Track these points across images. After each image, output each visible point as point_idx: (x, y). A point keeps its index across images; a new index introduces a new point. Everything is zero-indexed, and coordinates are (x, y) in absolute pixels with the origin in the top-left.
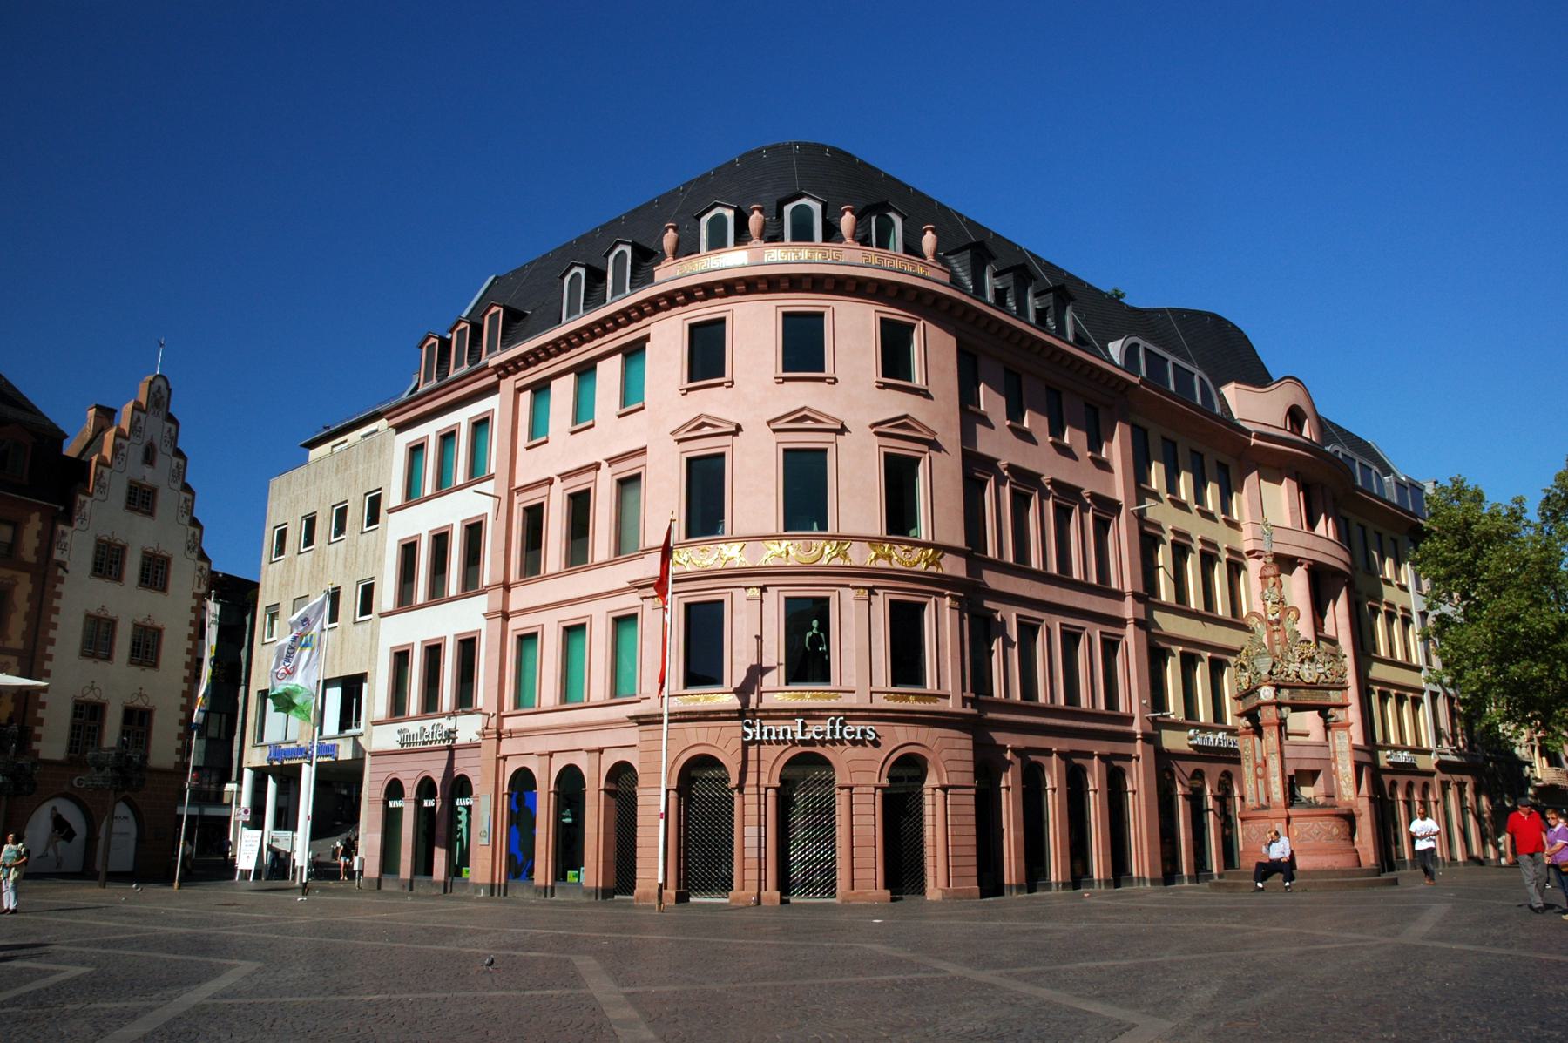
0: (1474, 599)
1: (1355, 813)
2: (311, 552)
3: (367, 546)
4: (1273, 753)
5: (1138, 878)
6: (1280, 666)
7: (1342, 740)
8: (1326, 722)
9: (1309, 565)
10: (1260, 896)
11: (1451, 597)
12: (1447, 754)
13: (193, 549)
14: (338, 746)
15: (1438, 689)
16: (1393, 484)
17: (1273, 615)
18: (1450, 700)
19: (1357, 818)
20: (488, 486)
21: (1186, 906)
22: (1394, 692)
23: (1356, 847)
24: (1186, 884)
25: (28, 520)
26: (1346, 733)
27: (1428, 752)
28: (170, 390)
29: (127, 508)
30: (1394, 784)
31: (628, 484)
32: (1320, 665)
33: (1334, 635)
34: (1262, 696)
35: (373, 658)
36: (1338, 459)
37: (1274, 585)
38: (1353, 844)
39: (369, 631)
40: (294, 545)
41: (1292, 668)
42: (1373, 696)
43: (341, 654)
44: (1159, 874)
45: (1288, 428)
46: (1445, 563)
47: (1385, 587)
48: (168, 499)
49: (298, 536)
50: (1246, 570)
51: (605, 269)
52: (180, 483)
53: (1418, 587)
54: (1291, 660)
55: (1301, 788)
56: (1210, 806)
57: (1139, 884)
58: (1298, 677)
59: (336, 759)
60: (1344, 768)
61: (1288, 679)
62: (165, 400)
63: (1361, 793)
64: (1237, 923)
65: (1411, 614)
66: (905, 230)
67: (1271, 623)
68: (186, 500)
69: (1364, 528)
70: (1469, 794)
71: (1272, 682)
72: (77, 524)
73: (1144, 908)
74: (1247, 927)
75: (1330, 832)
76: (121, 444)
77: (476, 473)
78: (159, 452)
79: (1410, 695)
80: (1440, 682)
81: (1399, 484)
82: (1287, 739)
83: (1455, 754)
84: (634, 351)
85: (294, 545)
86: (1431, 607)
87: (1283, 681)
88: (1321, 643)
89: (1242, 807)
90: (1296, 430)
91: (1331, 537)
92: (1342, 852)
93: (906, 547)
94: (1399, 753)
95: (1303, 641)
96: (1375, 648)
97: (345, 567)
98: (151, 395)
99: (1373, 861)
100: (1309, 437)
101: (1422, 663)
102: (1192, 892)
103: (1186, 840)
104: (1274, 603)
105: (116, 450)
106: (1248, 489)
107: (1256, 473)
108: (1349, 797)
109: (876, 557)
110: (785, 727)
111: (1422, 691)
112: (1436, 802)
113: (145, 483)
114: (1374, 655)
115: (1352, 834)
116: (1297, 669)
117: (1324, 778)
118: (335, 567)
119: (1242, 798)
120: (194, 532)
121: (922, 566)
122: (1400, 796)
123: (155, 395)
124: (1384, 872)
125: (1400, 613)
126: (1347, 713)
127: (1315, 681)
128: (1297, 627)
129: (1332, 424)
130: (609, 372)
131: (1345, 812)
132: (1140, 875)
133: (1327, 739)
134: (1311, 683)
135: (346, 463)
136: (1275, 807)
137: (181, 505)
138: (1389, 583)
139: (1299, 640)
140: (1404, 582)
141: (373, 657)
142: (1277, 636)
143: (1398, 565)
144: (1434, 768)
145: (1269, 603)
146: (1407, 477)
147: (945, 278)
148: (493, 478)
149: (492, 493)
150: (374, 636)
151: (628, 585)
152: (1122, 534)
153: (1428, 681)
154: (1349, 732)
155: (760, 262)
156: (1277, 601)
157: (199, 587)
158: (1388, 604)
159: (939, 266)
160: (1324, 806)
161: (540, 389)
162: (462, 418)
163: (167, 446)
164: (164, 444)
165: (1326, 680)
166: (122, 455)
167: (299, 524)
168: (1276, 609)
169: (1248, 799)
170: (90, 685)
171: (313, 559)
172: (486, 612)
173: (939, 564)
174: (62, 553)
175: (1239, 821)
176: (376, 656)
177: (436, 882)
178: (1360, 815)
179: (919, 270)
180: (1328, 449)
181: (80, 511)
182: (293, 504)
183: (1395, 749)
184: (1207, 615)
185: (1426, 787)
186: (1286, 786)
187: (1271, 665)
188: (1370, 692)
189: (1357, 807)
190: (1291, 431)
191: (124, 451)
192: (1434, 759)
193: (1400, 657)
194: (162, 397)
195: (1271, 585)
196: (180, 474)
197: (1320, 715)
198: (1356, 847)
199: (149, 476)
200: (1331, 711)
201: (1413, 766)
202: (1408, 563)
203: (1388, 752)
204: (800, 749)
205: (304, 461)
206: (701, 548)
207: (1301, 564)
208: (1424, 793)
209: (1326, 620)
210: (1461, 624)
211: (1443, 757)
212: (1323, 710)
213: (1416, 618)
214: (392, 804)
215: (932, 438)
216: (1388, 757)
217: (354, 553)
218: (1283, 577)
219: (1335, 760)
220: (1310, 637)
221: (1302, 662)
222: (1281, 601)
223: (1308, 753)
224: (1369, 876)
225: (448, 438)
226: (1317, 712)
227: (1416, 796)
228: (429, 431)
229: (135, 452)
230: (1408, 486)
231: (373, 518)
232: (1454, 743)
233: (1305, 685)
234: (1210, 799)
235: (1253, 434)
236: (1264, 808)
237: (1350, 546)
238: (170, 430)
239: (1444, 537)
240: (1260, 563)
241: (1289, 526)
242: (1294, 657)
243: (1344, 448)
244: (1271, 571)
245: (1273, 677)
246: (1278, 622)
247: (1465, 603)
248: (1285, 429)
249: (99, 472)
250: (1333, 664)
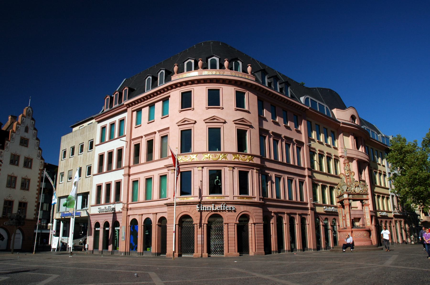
0: (403, 169)
1: (371, 229)
2: (73, 157)
3: (89, 155)
5: (310, 249)
8: (362, 204)
9: (357, 160)
10: (344, 253)
11: (397, 168)
12: (396, 213)
13: (39, 156)
14: (81, 212)
15: (393, 194)
16: (381, 137)
17: (347, 174)
18: (397, 197)
19: (371, 231)
20: (124, 139)
21: (323, 257)
22: (381, 195)
23: (371, 239)
24: (323, 250)
26: (368, 207)
27: (391, 212)
29: (20, 145)
30: (381, 221)
31: (164, 138)
32: (360, 188)
33: (365, 179)
34: (344, 197)
35: (91, 188)
36: (365, 130)
37: (347, 165)
38: (370, 238)
39: (90, 179)
41: (353, 189)
42: (375, 197)
43: (82, 186)
44: (316, 247)
45: (351, 121)
46: (396, 159)
47: (379, 166)
48: (32, 142)
49: (69, 153)
50: (339, 161)
52: (35, 138)
53: (388, 166)
54: (352, 186)
55: (356, 223)
56: (330, 228)
57: (310, 250)
58: (354, 191)
59: (80, 216)
60: (368, 217)
61: (351, 192)
62: (31, 114)
63: (372, 224)
64: (338, 261)
65: (386, 173)
66: (242, 66)
67: (347, 176)
68: (37, 142)
69: (373, 149)
70: (403, 223)
71: (347, 193)
72: (5, 149)
73: (312, 257)
74: (340, 262)
75: (364, 235)
77: (121, 135)
78: (29, 129)
79: (386, 196)
80: (394, 192)
81: (382, 137)
82: (351, 209)
83: (399, 213)
84: (166, 100)
86: (392, 171)
87: (350, 192)
88: (361, 182)
89: (339, 228)
90: (353, 122)
91: (363, 152)
92: (367, 241)
93: (243, 155)
94: (383, 213)
95: (356, 181)
96: (376, 183)
97: (83, 161)
99: (376, 243)
100: (357, 124)
101: (389, 187)
102: (325, 252)
103: (323, 238)
104: (347, 171)
105: (17, 128)
106: (340, 138)
107: (342, 134)
108: (369, 225)
109: (235, 158)
111: (389, 195)
112: (394, 226)
114: (376, 185)
115: (370, 236)
117: (362, 220)
119: (339, 226)
120: (40, 152)
121: (248, 161)
122: (383, 225)
123: (28, 113)
124: (379, 246)
125: (383, 173)
126: (368, 201)
127: (359, 193)
128: (354, 177)
129: (363, 120)
130: (159, 106)
131: (368, 229)
132: (310, 248)
133: (363, 209)
134: (358, 193)
135: (83, 132)
136: (348, 228)
138: (380, 165)
139: (355, 181)
140: (384, 164)
141: (91, 187)
142: (348, 180)
143: (382, 159)
144: (393, 217)
145: (346, 171)
146: (384, 135)
147: (254, 79)
148: (125, 136)
149: (125, 140)
150: (92, 181)
151: (164, 166)
152: (304, 151)
153: (391, 192)
154: (369, 207)
155: (202, 75)
157: (41, 167)
158: (379, 171)
159: (252, 76)
160: (362, 228)
161: (139, 111)
162: (117, 119)
164: (31, 126)
167: (70, 149)
169: (340, 226)
170: (9, 195)
171: (74, 159)
172: (123, 174)
173: (252, 160)
175: (338, 232)
176: (92, 187)
178: (372, 230)
179: (247, 77)
180: (362, 127)
181: (6, 146)
183: (382, 211)
184: (328, 174)
185: (391, 222)
186: (351, 222)
187: (347, 188)
188: (374, 195)
189: (371, 228)
190: (352, 122)
191: (19, 128)
192: (393, 214)
193: (383, 185)
194: (30, 113)
195: (346, 165)
197: (361, 202)
198: (371, 239)
199: (26, 136)
200: (364, 201)
201: (387, 216)
202: (385, 159)
203: (380, 212)
204: (213, 213)
205: (71, 131)
206: (185, 156)
207: (355, 160)
208: (390, 224)
209: (362, 175)
210: (400, 176)
211: (395, 214)
212: (361, 201)
213: (387, 174)
214: (96, 229)
215: (250, 125)
216: (380, 214)
217: (86, 157)
218: (350, 163)
219: (365, 215)
220: (358, 180)
221: (356, 187)
222: (350, 170)
223: (357, 213)
224: (375, 247)
225: (112, 125)
226: (360, 201)
227: (388, 225)
228: (107, 123)
229: (22, 129)
230: (385, 137)
231: (91, 148)
232: (398, 209)
233: (356, 193)
234: (330, 226)
235: (341, 123)
236: (345, 228)
237: (369, 154)
238: (32, 123)
239: (395, 152)
240: (343, 159)
241: (352, 149)
242: (353, 186)
243: (367, 127)
244: (347, 162)
245: (348, 192)
246: (349, 176)
247: (401, 170)
248: (350, 122)
249: (12, 134)
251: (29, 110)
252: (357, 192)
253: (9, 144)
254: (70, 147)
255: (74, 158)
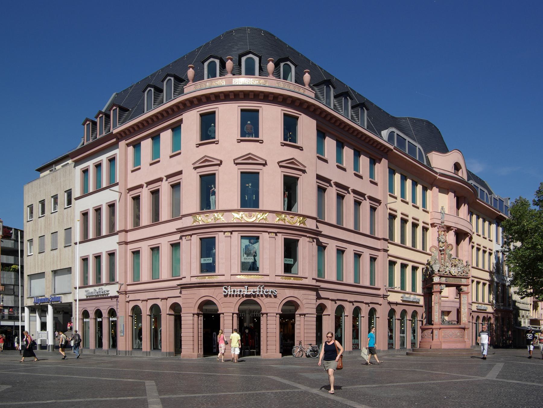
3: (67, 214)
4: (437, 303)
6: (443, 268)
7: (465, 299)
14: (62, 297)
20: (116, 188)
26: (466, 296)
31: (176, 186)
34: (434, 280)
35: (74, 261)
39: (71, 250)
40: (36, 214)
43: (60, 260)
49: (38, 210)
51: (162, 89)
58: (450, 273)
60: (464, 310)
61: (445, 273)
66: (296, 73)
71: (439, 275)
77: (112, 184)
84: (176, 128)
85: (36, 214)
87: (444, 274)
93: (291, 216)
97: (59, 223)
109: (279, 220)
110: (241, 289)
116: (450, 270)
118: (55, 223)
121: (298, 224)
126: (468, 288)
127: (456, 275)
130: (166, 137)
135: (56, 178)
139: (452, 257)
147: (313, 95)
148: (118, 185)
149: (118, 191)
150: (73, 252)
151: (176, 230)
152: (381, 214)
155: (231, 84)
156: (444, 241)
159: (310, 89)
161: (136, 145)
162: (104, 158)
165: (461, 274)
167: (38, 205)
168: (444, 245)
172: (118, 242)
173: (304, 223)
177: (104, 350)
179: (301, 91)
182: (34, 196)
184: (413, 248)
204: (245, 299)
205: (38, 178)
206: (206, 215)
212: (458, 287)
214: (85, 320)
215: (304, 169)
217: (62, 217)
223: (447, 304)
225: (98, 166)
228: (90, 164)
231: (69, 202)
233: (451, 276)
245: (440, 273)
250: (465, 268)
252: (453, 275)
254: (38, 201)
255: (45, 218)
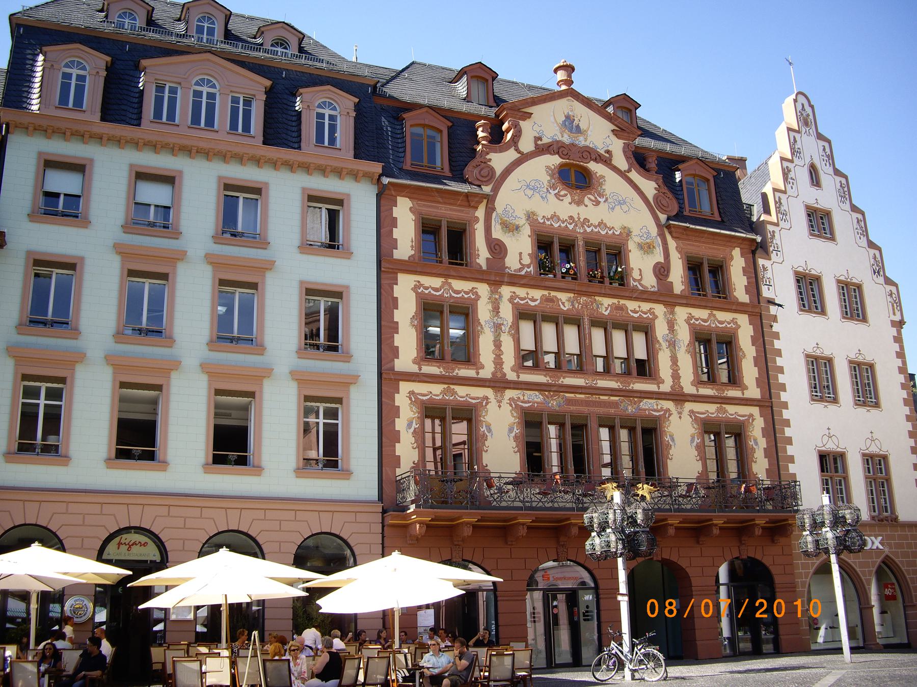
13: (879, 272)
25: (732, 259)
28: (812, 107)
48: (842, 221)
52: (848, 202)
62: (811, 117)
72: (773, 255)
76: (787, 167)
98: (799, 114)
105: (786, 173)
113: (819, 206)
120: (874, 254)
123: (802, 114)
137: (855, 227)
163: (826, 165)
164: (823, 163)
166: (792, 178)
174: (769, 290)
181: (772, 242)
194: (808, 115)
196: (845, 193)
229: (802, 175)
238: (824, 150)
251: (803, 105)
253: (777, 235)
